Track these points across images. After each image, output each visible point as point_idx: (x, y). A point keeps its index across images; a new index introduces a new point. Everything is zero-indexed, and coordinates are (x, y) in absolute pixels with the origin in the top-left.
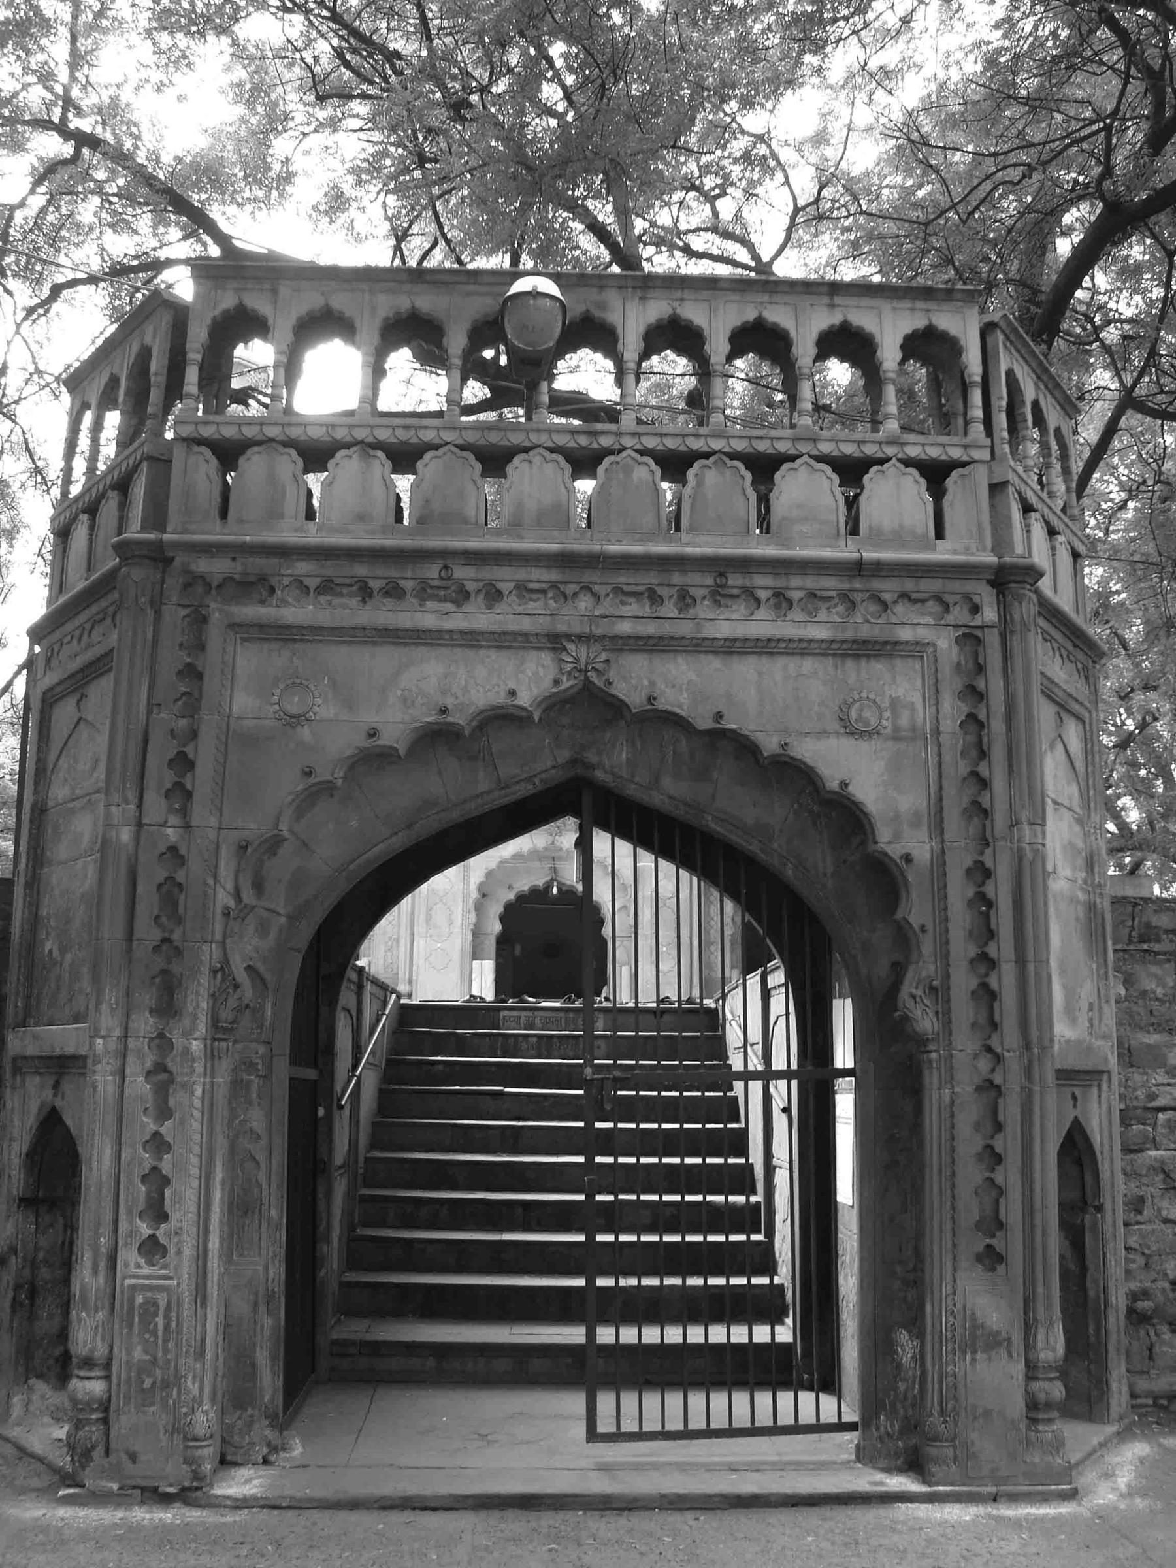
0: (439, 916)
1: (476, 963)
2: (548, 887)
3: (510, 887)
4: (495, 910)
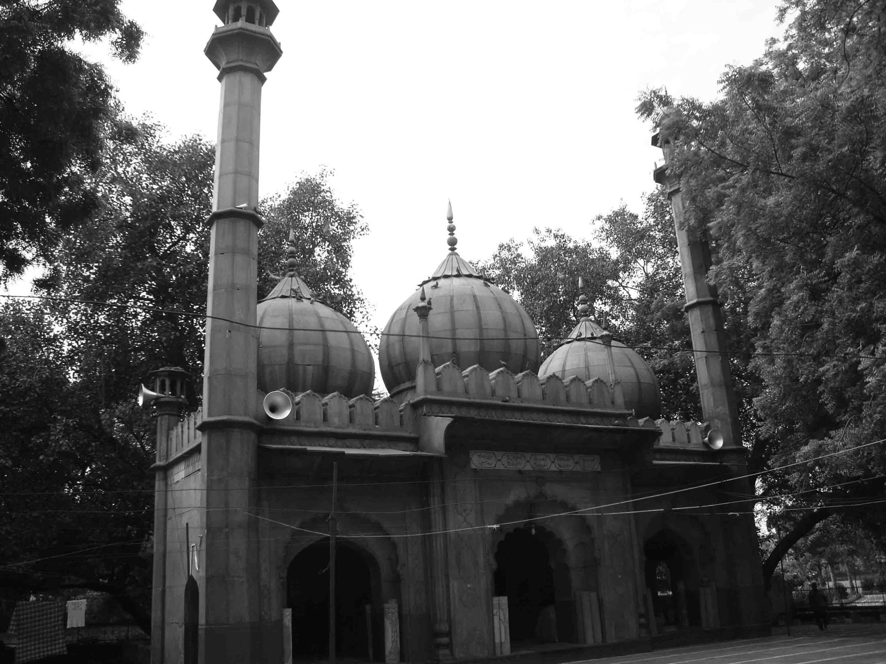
1: (496, 600)
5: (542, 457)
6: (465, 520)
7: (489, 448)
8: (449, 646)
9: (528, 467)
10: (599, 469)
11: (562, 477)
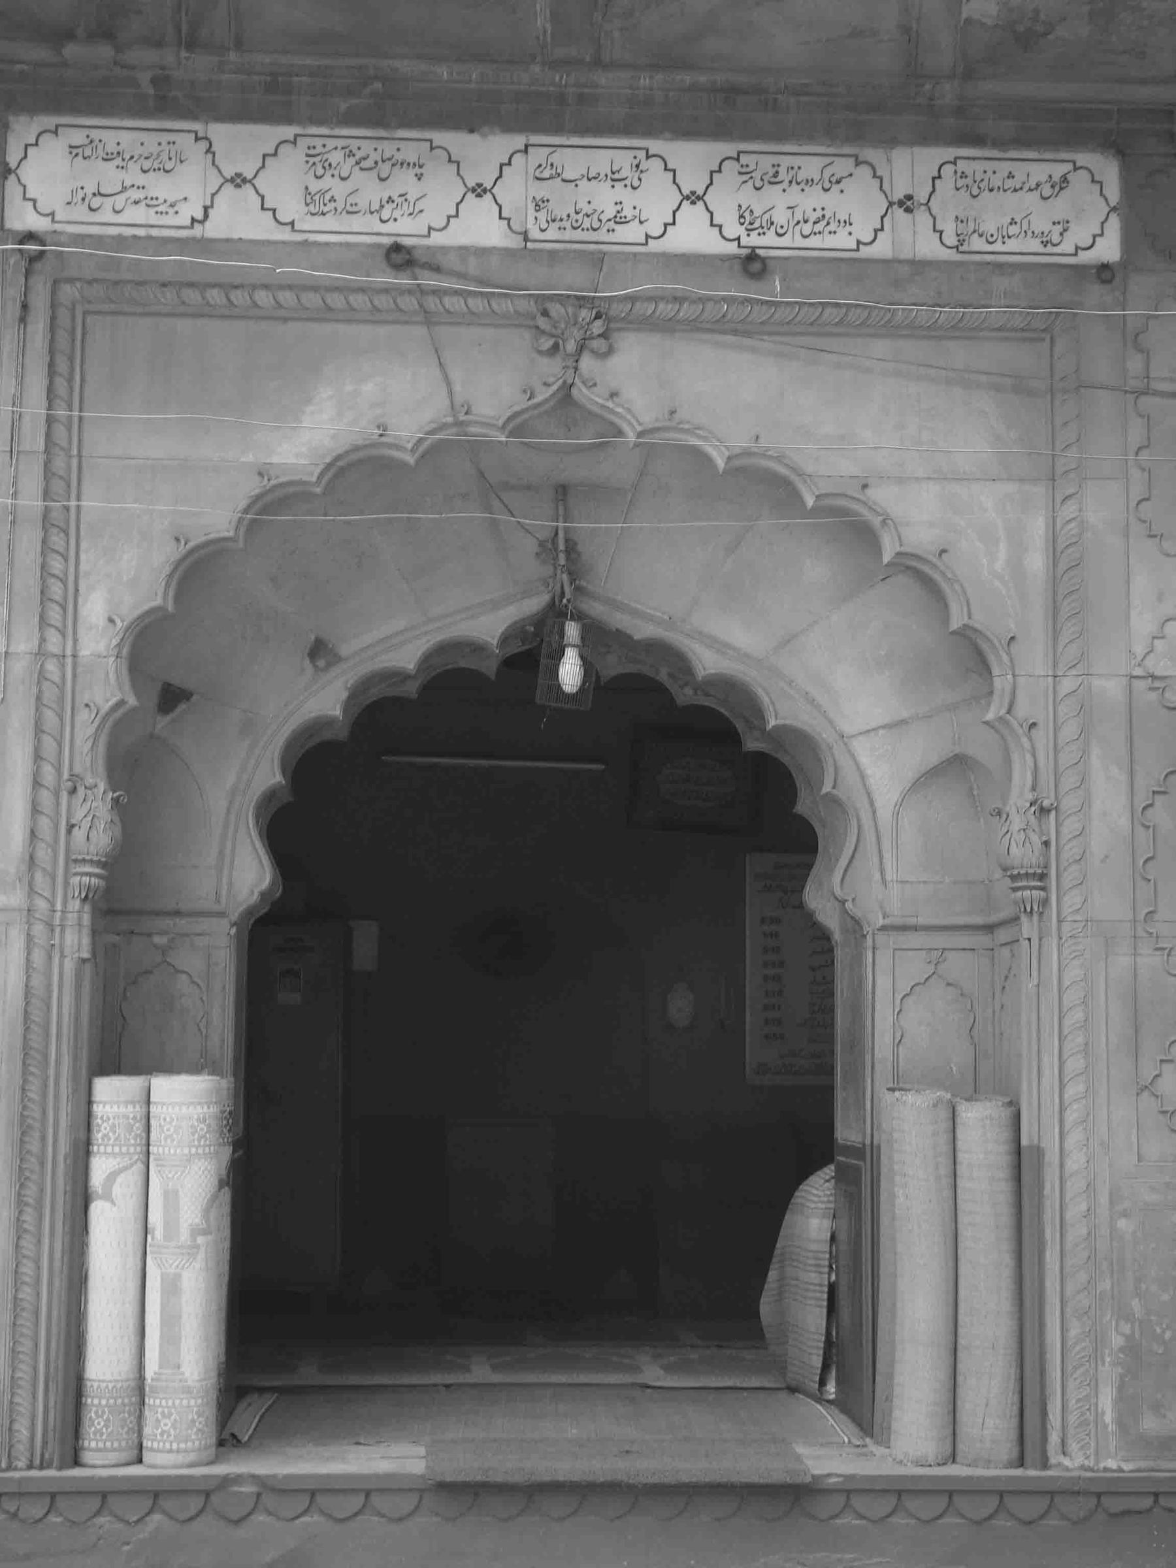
1: (113, 1095)
2: (530, 654)
3: (320, 651)
5: (601, 161)
7: (167, 101)
9: (480, 228)
10: (1109, 249)
11: (752, 297)
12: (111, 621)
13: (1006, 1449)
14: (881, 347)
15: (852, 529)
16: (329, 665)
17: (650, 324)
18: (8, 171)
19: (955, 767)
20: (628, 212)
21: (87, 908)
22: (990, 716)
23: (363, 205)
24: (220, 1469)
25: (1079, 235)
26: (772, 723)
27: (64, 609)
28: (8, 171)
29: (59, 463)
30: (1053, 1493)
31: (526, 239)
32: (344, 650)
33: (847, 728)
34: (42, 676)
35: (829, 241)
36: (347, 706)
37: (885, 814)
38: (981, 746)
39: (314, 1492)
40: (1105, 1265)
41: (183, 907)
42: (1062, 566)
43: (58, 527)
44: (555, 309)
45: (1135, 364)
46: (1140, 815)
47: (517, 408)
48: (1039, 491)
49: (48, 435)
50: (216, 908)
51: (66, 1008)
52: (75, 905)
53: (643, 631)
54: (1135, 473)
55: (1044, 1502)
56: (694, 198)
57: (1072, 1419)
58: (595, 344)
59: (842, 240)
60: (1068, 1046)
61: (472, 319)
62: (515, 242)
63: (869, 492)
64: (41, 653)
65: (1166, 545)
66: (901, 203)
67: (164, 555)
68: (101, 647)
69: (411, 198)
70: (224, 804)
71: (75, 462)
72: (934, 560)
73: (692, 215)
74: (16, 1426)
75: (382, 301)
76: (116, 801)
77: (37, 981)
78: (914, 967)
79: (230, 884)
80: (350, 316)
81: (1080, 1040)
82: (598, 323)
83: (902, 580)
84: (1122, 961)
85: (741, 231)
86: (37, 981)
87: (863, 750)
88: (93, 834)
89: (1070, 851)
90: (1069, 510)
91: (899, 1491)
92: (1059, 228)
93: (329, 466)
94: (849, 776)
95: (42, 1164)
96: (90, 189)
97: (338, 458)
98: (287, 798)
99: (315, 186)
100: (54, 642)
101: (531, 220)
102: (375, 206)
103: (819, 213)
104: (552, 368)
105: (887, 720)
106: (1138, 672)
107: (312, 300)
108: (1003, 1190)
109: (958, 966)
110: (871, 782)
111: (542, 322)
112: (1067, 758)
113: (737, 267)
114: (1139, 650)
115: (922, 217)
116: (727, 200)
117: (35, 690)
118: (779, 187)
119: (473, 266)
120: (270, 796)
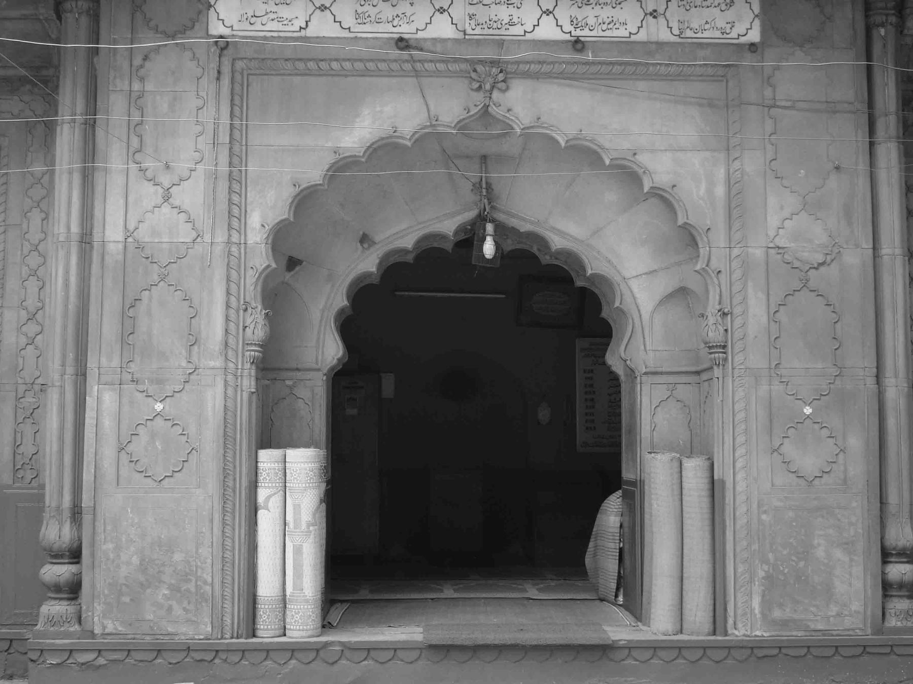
0: (160, 323)
1: (268, 458)
2: (469, 240)
3: (365, 240)
4: (323, 304)
6: (167, 198)
8: (73, 590)
9: (443, 29)
12: (263, 226)
13: (707, 627)
14: (642, 85)
15: (628, 175)
16: (370, 246)
17: (527, 75)
18: (210, 6)
19: (682, 293)
20: (515, 20)
21: (254, 367)
22: (698, 267)
23: (384, 19)
24: (324, 639)
25: (740, 29)
26: (589, 272)
27: (240, 220)
28: (210, 6)
29: (236, 148)
30: (729, 648)
31: (465, 34)
32: (377, 239)
33: (627, 274)
34: (230, 254)
35: (616, 33)
36: (380, 264)
37: (646, 316)
38: (694, 283)
39: (369, 650)
40: (756, 538)
41: (299, 366)
42: (733, 192)
43: (236, 180)
44: (480, 68)
45: (768, 92)
46: (773, 316)
47: (462, 117)
48: (722, 156)
49: (231, 135)
50: (315, 366)
51: (245, 415)
52: (248, 366)
53: (524, 227)
54: (769, 147)
55: (725, 652)
56: (548, 12)
57: (739, 612)
58: (499, 85)
59: (622, 32)
60: (737, 430)
61: (438, 74)
62: (460, 36)
63: (637, 156)
64: (229, 242)
65: (785, 183)
66: (651, 14)
67: (288, 193)
68: (258, 239)
69: (408, 14)
70: (319, 314)
71: (244, 148)
72: (670, 191)
73: (547, 20)
74: (225, 618)
75: (395, 66)
76: (267, 314)
77: (230, 404)
78: (661, 392)
79: (323, 353)
80: (378, 73)
81: (743, 427)
82: (501, 75)
83: (654, 201)
84: (764, 388)
85: (572, 29)
86: (230, 404)
87: (635, 285)
88: (256, 331)
89: (737, 335)
90: (737, 165)
91: (655, 648)
92: (729, 26)
93: (369, 147)
94: (628, 299)
95: (234, 491)
96: (249, 15)
97: (373, 144)
98: (349, 312)
99: (360, 10)
100: (235, 238)
101: (467, 25)
102: (390, 19)
103: (610, 19)
104: (479, 97)
105: (646, 270)
106: (771, 245)
107: (359, 66)
108: (706, 502)
109: (683, 392)
110: (639, 301)
111: (473, 75)
112: (737, 287)
113: (570, 46)
114: (772, 233)
115: (662, 20)
116: (564, 14)
117: (226, 260)
118: (590, 7)
119: (439, 48)
120: (341, 311)
